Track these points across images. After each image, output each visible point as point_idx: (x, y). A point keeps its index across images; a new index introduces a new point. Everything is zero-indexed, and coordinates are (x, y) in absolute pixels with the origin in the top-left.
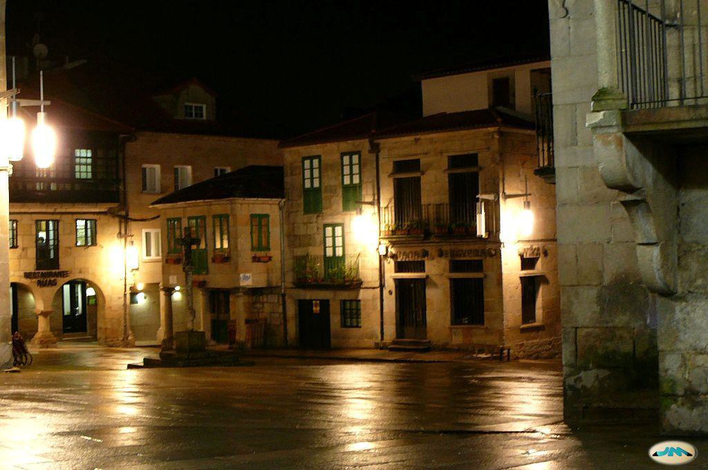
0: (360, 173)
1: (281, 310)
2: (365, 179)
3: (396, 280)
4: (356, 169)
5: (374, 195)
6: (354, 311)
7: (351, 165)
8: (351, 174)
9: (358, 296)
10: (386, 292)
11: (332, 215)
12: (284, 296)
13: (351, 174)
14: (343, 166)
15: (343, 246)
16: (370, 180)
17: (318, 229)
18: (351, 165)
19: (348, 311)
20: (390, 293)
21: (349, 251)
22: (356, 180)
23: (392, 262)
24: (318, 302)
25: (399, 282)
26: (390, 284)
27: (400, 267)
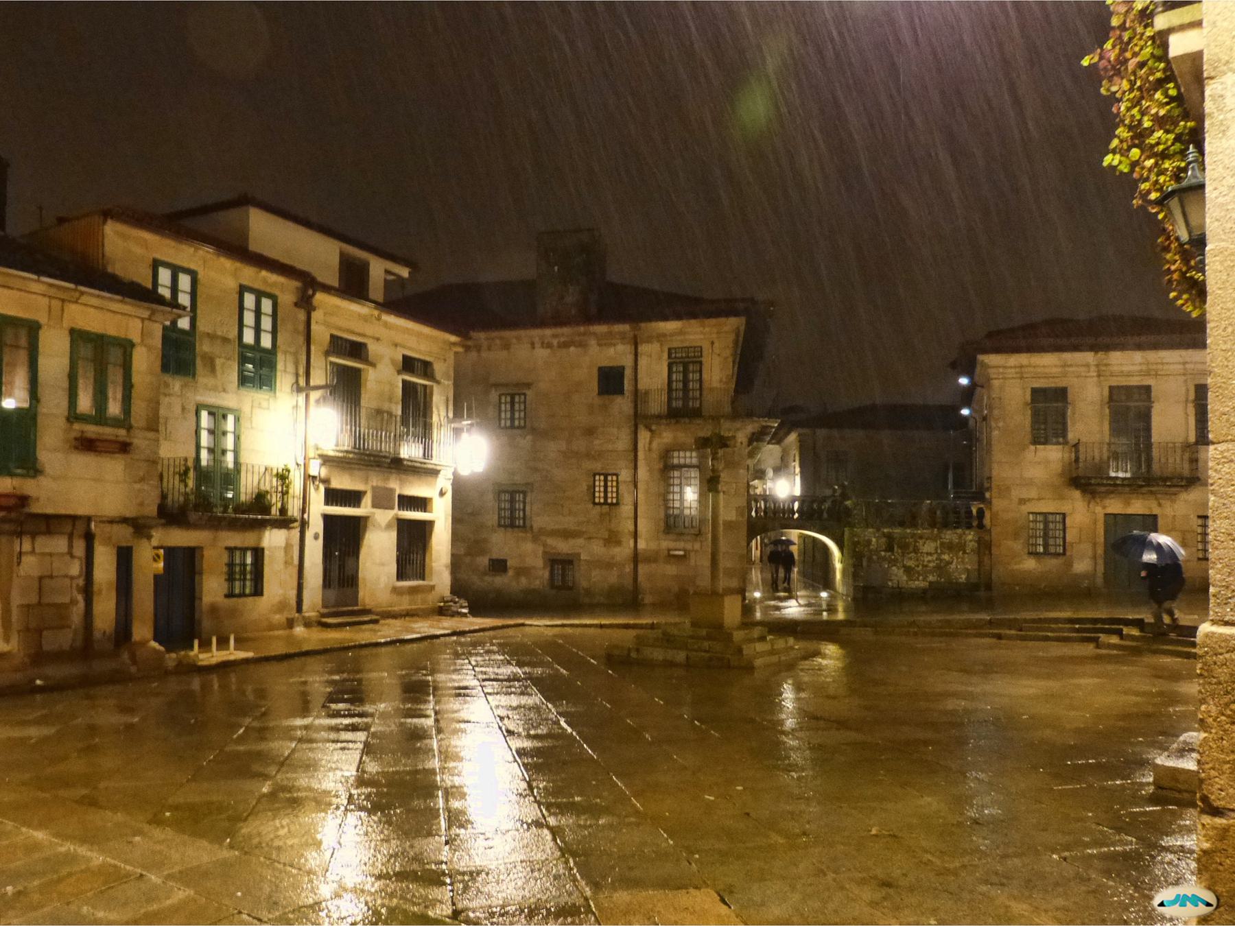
0: (274, 332)
1: (75, 569)
2: (279, 342)
3: (327, 519)
4: (266, 323)
5: (297, 375)
6: (237, 569)
7: (258, 313)
8: (258, 330)
9: (260, 539)
10: (309, 535)
11: (214, 389)
12: (89, 538)
13: (258, 330)
14: (241, 309)
15: (236, 452)
16: (292, 350)
17: (183, 409)
18: (258, 313)
19: (237, 569)
20: (316, 537)
21: (244, 459)
22: (266, 342)
23: (322, 488)
24: (162, 551)
25: (327, 519)
26: (316, 526)
27: (333, 496)
